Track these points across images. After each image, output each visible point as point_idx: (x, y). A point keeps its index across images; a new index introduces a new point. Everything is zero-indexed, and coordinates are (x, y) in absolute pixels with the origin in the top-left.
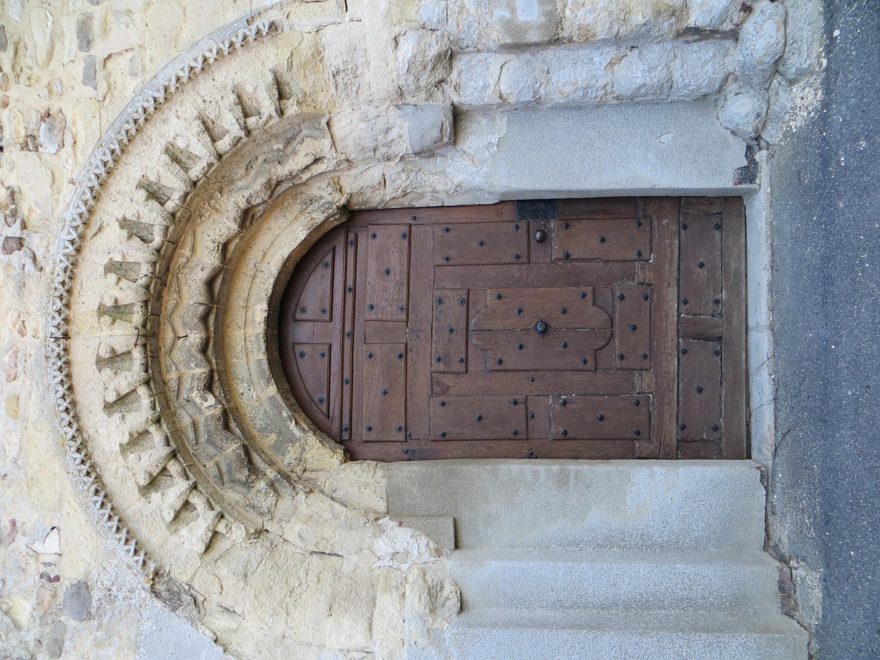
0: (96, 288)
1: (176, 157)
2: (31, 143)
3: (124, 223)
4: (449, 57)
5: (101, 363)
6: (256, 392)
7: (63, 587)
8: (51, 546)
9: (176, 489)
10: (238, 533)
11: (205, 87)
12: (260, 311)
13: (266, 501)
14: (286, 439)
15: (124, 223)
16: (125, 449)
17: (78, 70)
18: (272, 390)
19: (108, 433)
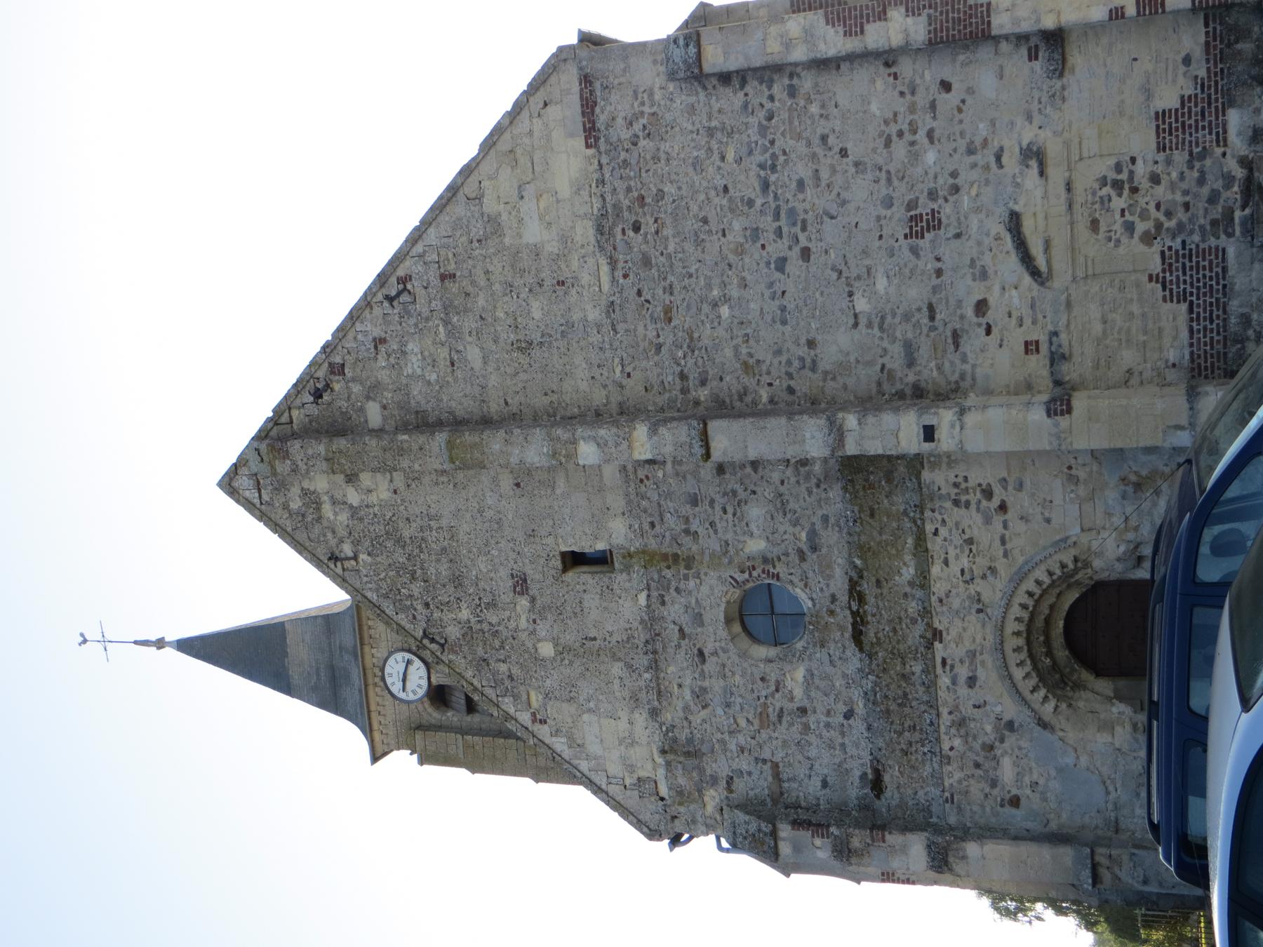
0: (1011, 626)
1: (1038, 582)
2: (984, 577)
3: (1020, 605)
4: (1136, 547)
5: (1014, 650)
6: (1062, 654)
7: (1002, 723)
8: (999, 709)
9: (1043, 692)
10: (1064, 706)
11: (1049, 561)
12: (1061, 624)
13: (1070, 694)
14: (1073, 670)
15: (1020, 605)
16: (1024, 678)
17: (1001, 553)
18: (1067, 653)
19: (1018, 674)
